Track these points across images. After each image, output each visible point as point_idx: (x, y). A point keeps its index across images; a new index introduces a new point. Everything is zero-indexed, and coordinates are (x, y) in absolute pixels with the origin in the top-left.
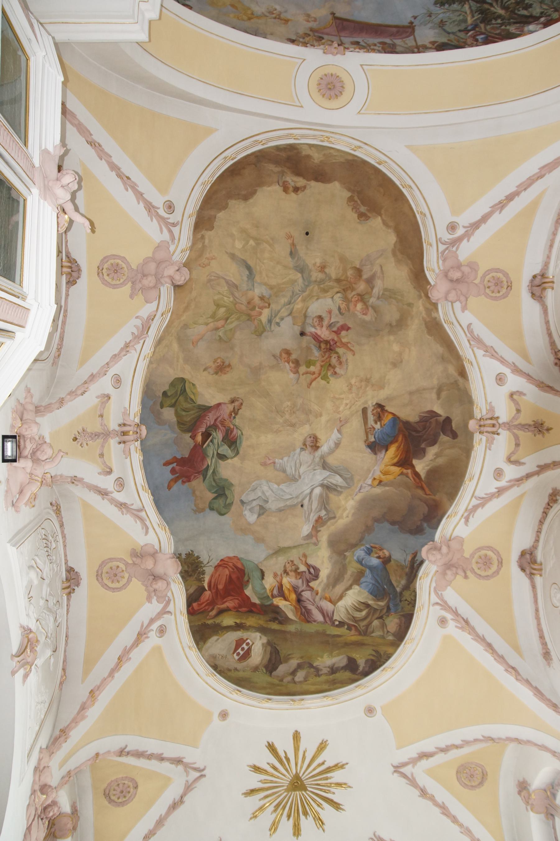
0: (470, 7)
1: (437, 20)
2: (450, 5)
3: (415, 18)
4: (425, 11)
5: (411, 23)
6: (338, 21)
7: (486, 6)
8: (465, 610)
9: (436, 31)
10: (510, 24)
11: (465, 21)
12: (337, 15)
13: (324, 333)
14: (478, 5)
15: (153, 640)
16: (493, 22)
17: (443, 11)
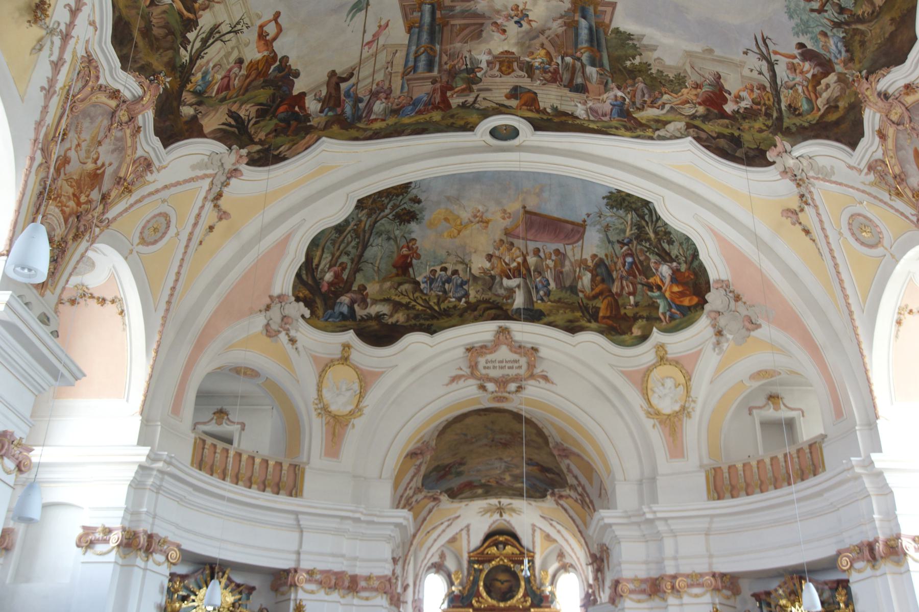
0: (632, 218)
1: (604, 223)
2: (618, 210)
3: (588, 215)
4: (597, 210)
5: (584, 221)
6: (528, 216)
7: (644, 223)
8: (566, 506)
9: (601, 236)
10: (653, 253)
11: (624, 231)
12: (528, 208)
13: (503, 441)
14: (638, 219)
15: (435, 508)
16: (643, 243)
17: (611, 214)
